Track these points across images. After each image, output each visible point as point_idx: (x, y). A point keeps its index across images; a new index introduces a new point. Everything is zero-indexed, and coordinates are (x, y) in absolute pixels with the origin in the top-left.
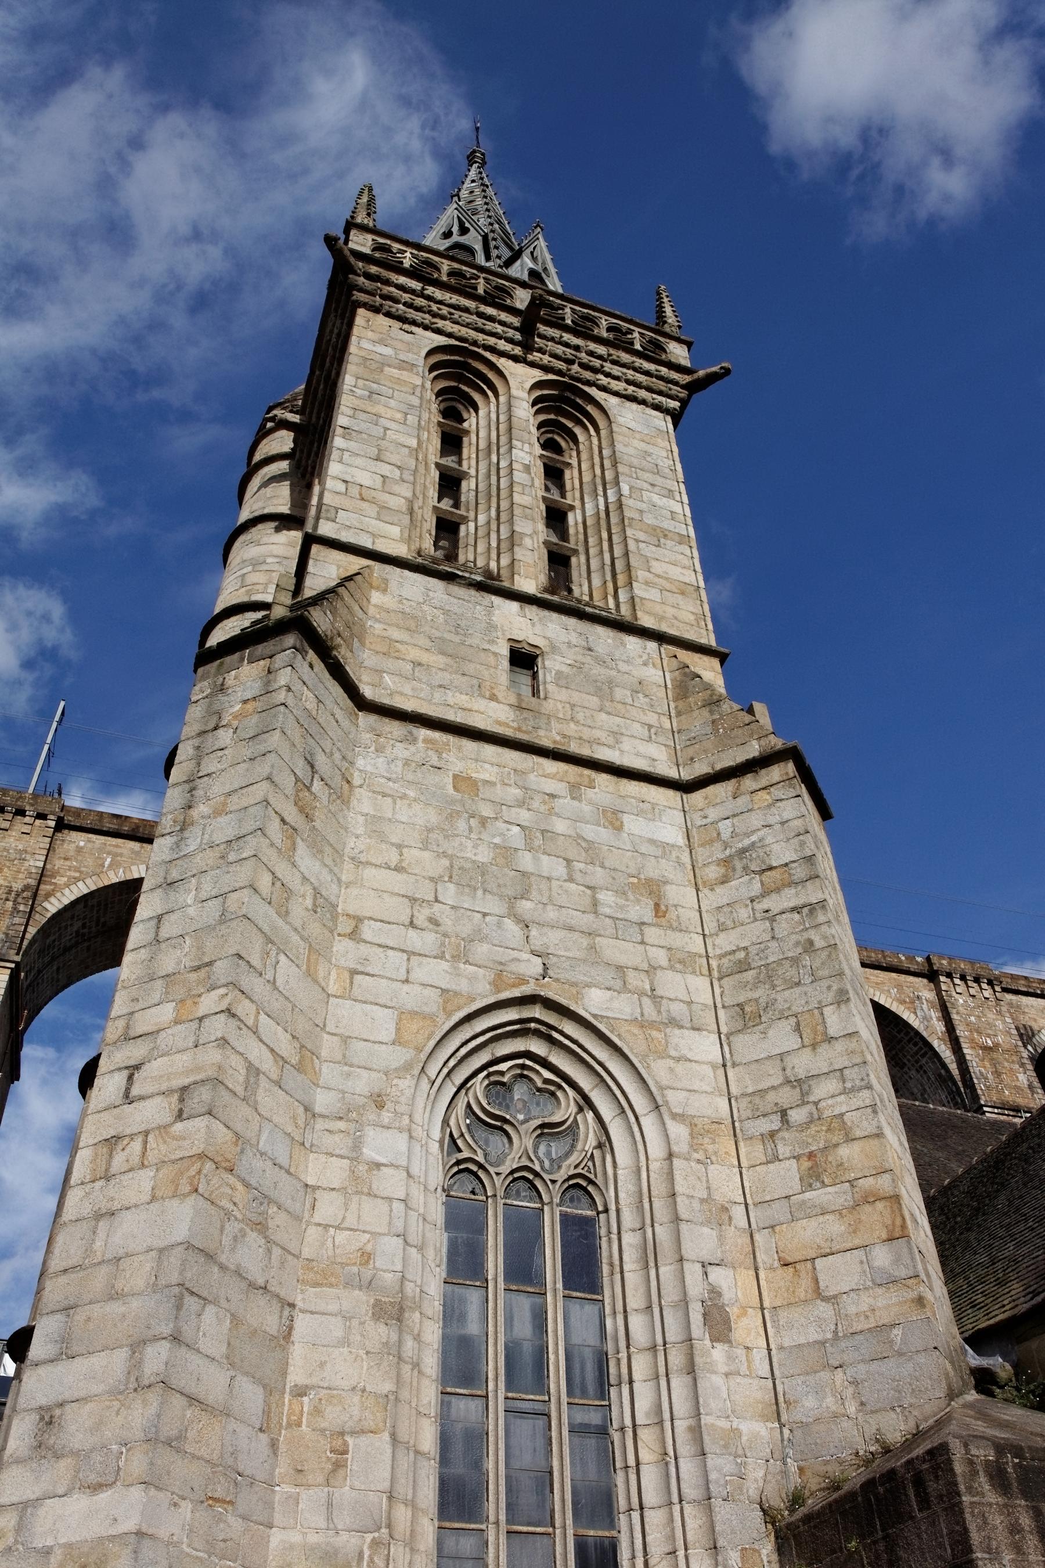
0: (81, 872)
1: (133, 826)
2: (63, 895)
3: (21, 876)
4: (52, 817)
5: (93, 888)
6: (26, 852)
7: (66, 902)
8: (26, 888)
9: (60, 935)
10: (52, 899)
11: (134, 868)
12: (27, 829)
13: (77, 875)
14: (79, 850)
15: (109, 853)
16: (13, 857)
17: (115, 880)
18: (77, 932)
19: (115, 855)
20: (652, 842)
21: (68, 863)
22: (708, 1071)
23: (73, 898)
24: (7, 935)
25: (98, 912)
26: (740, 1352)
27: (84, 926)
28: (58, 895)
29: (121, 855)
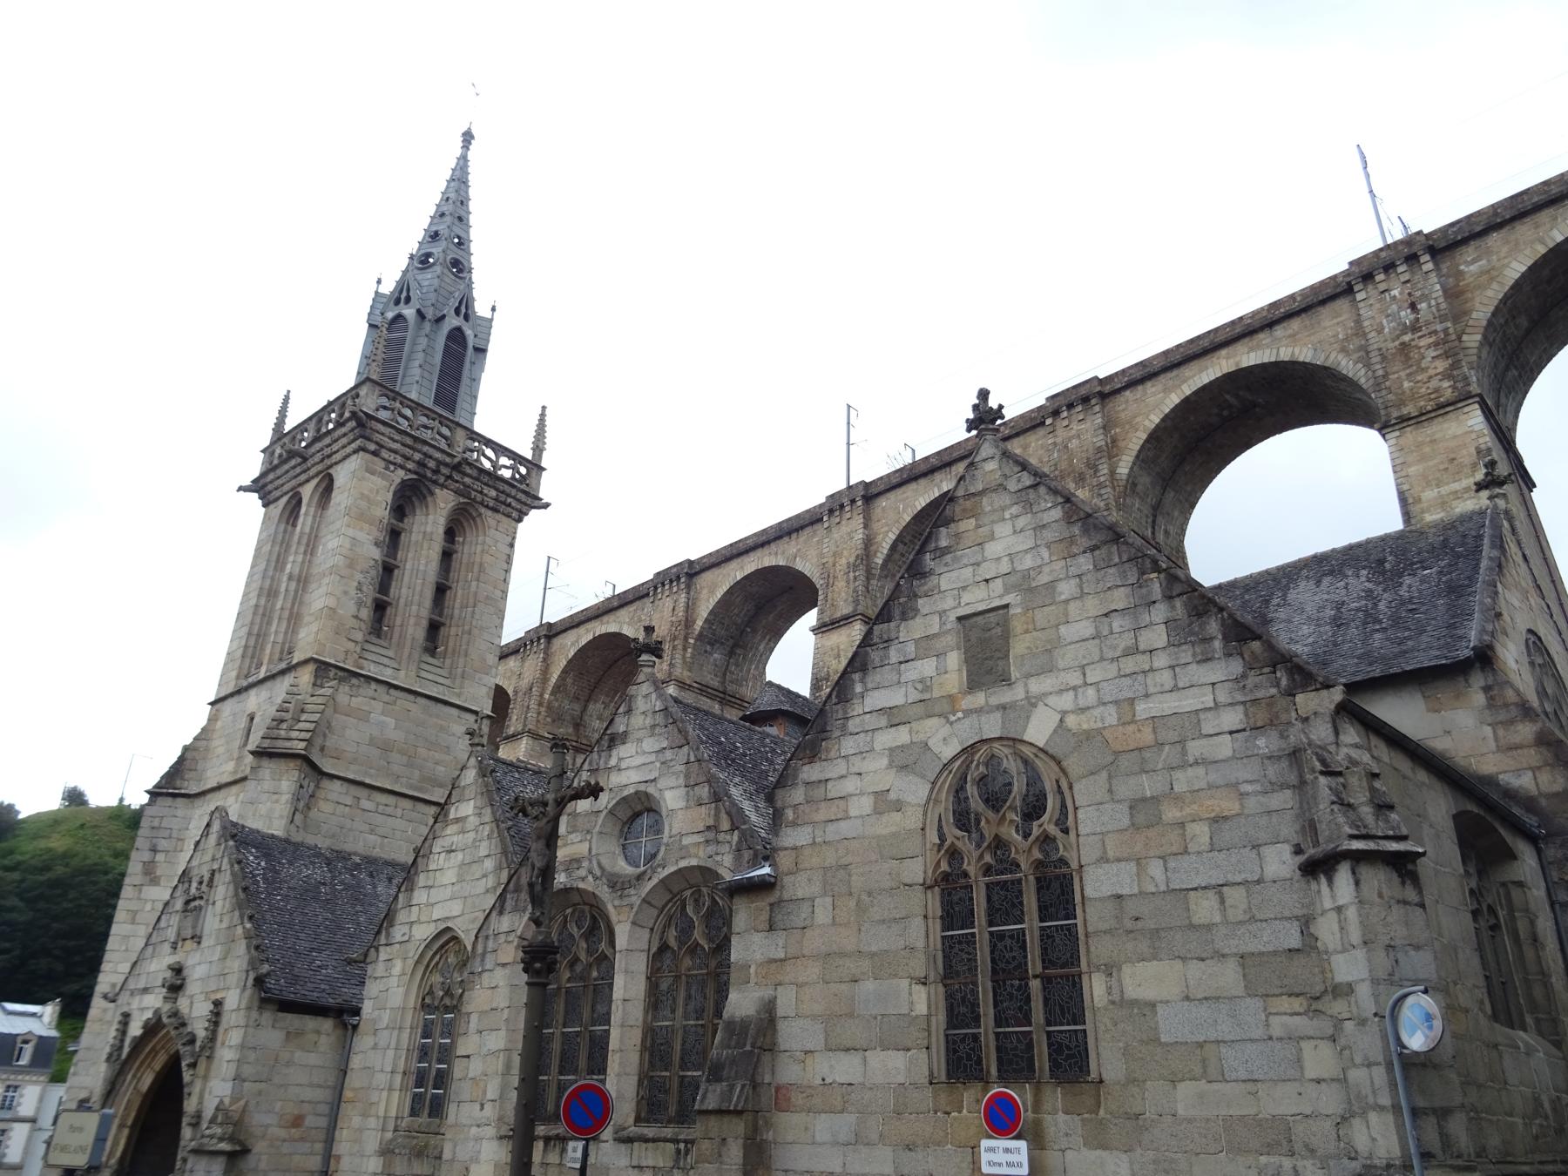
12: (848, 515)
14: (884, 509)
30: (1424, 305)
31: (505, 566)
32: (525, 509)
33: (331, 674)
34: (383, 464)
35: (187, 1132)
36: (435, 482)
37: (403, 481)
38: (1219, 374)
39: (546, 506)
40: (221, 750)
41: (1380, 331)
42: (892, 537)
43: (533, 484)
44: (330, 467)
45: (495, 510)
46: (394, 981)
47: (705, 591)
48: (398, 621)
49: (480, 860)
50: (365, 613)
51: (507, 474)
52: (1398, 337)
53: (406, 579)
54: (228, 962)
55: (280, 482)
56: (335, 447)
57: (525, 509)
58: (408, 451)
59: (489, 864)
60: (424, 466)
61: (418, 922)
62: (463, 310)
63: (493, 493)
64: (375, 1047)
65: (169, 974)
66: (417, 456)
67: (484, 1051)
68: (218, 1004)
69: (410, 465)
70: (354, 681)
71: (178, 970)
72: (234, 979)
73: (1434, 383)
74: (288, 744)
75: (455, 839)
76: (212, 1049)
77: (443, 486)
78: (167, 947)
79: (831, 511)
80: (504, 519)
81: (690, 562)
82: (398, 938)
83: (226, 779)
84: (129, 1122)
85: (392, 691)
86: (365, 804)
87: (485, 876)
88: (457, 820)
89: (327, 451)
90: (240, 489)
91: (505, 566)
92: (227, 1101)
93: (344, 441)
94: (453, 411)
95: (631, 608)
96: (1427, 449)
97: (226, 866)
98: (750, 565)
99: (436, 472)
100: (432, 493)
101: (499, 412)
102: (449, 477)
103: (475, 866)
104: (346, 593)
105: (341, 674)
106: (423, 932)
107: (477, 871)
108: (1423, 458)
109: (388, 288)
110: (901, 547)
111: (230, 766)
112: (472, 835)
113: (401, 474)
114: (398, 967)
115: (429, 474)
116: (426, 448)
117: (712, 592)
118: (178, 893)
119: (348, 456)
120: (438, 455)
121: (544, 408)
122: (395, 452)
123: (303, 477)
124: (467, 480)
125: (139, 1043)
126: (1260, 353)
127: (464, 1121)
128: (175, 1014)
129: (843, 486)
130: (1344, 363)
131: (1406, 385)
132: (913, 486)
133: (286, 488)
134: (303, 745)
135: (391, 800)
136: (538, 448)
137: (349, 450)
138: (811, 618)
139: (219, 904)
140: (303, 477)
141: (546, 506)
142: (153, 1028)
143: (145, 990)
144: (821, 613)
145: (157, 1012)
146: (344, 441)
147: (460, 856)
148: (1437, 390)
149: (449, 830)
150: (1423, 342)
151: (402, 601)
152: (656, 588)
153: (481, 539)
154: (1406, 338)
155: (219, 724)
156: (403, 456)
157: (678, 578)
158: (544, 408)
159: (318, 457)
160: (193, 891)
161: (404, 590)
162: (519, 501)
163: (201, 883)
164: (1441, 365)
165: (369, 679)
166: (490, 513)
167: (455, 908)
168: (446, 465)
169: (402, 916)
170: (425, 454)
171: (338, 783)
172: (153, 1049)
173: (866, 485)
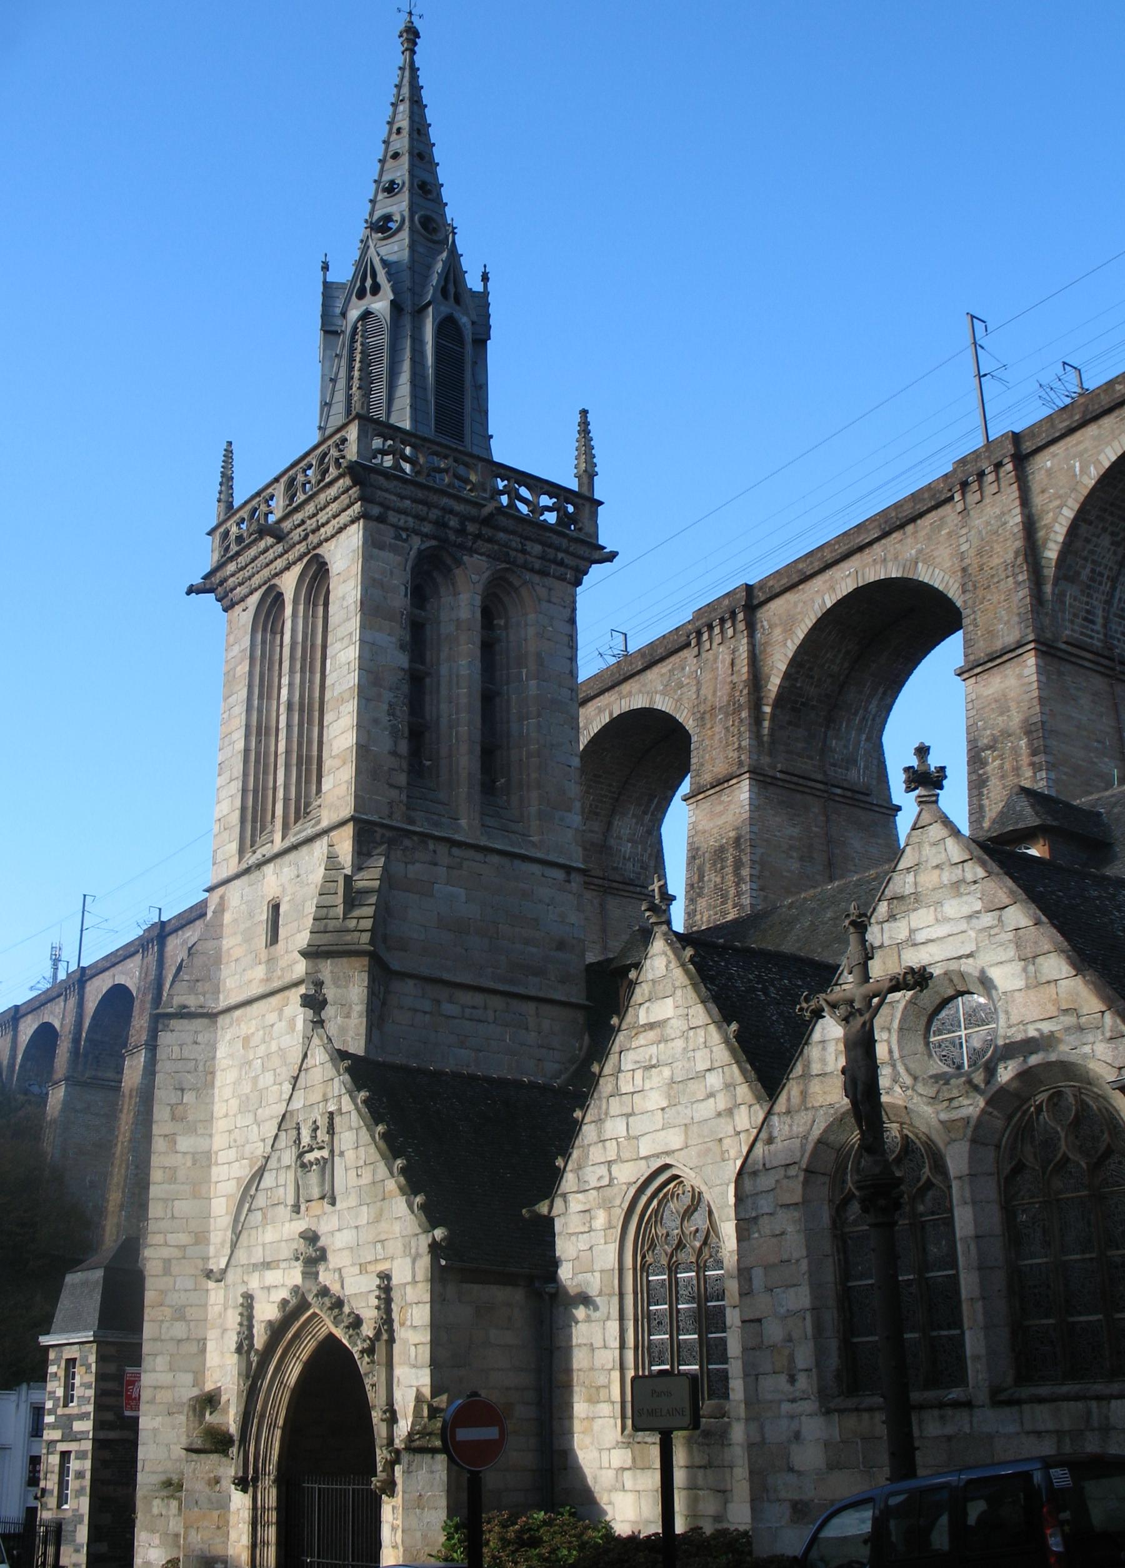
0: (1060, 497)
1: (1082, 409)
2: (1056, 532)
3: (1009, 543)
4: (1006, 460)
5: (1076, 507)
6: (1003, 514)
7: (1061, 539)
8: (1017, 554)
9: (1094, 562)
10: (1051, 545)
11: (1102, 457)
12: (994, 488)
13: (1057, 503)
14: (1049, 472)
15: (1074, 457)
16: (995, 527)
17: (1092, 483)
18: (1112, 544)
19: (1080, 455)
21: (1046, 495)
23: (1064, 530)
24: (1019, 614)
25: (1112, 514)
27: (1113, 534)
28: (1052, 535)
29: (1086, 450)
31: (568, 653)
32: (582, 564)
33: (378, 837)
34: (391, 532)
35: (380, 1430)
36: (461, 546)
37: (420, 552)
39: (612, 557)
40: (237, 952)
42: (1068, 514)
43: (588, 528)
44: (320, 544)
45: (543, 573)
46: (598, 1237)
47: (778, 631)
48: (444, 752)
49: (701, 1076)
50: (403, 747)
51: (551, 518)
53: (444, 691)
54: (384, 1225)
55: (246, 573)
56: (322, 517)
57: (582, 564)
58: (421, 509)
59: (714, 1080)
60: (445, 525)
61: (619, 1159)
62: (452, 290)
63: (537, 549)
65: (301, 1245)
66: (434, 514)
67: (782, 1310)
68: (385, 1277)
69: (427, 528)
70: (407, 842)
71: (311, 1238)
72: (395, 1247)
74: (348, 938)
76: (391, 1332)
77: (471, 551)
78: (284, 1212)
79: (964, 485)
80: (558, 584)
81: (749, 588)
82: (594, 1183)
83: (256, 990)
84: (281, 1423)
85: (456, 851)
86: (448, 1008)
87: (711, 1095)
88: (651, 1026)
89: (311, 524)
90: (191, 590)
91: (568, 653)
92: (427, 1392)
93: (334, 507)
94: (460, 438)
95: (663, 668)
97: (347, 1104)
98: (843, 581)
99: (462, 531)
100: (459, 563)
101: (525, 432)
102: (478, 536)
103: (693, 1086)
104: (376, 721)
105: (389, 834)
106: (629, 1174)
107: (697, 1089)
109: (343, 273)
110: (1084, 528)
111: (260, 972)
112: (679, 1044)
113: (416, 542)
114: (600, 1219)
115: (452, 537)
116: (445, 501)
117: (789, 631)
118: (282, 1142)
119: (340, 530)
120: (459, 507)
121: (584, 413)
122: (404, 512)
123: (279, 564)
124: (501, 535)
125: (277, 1330)
127: (769, 1397)
128: (324, 1292)
129: (978, 442)
132: (1092, 430)
133: (256, 580)
134: (366, 937)
135: (479, 999)
136: (588, 475)
137: (344, 518)
138: (950, 652)
139: (350, 1155)
140: (279, 564)
141: (612, 557)
142: (294, 1311)
143: (267, 1265)
144: (968, 643)
145: (296, 1290)
146: (334, 507)
147: (666, 1072)
149: (642, 1040)
151: (444, 721)
152: (699, 634)
153: (532, 617)
155: (227, 917)
156: (417, 517)
157: (733, 615)
158: (584, 413)
159: (296, 535)
160: (306, 1140)
161: (444, 706)
162: (572, 554)
163: (315, 1129)
165: (425, 837)
166: (536, 578)
167: (674, 1139)
168: (473, 519)
170: (443, 509)
171: (411, 982)
173: (1016, 438)
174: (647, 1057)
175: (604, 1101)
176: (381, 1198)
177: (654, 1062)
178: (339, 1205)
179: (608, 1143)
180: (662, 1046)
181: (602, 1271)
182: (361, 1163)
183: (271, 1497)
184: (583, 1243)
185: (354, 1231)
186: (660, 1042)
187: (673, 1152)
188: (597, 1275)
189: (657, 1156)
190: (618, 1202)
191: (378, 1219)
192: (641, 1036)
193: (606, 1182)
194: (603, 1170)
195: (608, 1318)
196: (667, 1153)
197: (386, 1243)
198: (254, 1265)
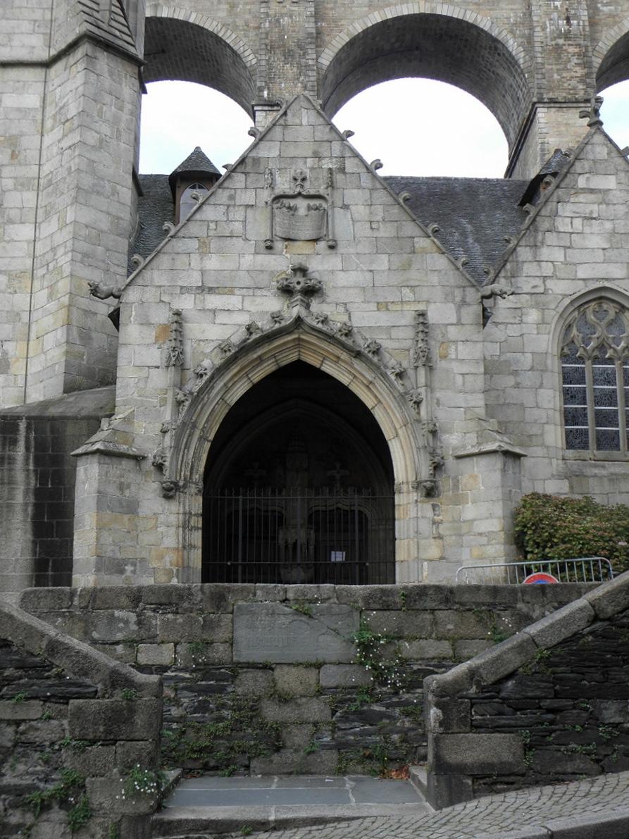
20: (19, 110)
22: (25, 245)
26: (12, 378)
30: (575, 22)
38: (417, 12)
41: (544, 29)
52: (555, 38)
64: (517, 386)
73: (573, 82)
75: (595, 207)
82: (527, 289)
84: (211, 437)
88: (592, 191)
96: (563, 129)
106: (564, 289)
108: (560, 134)
126: (451, 8)
130: (511, 42)
131: (556, 76)
148: (574, 89)
149: (582, 198)
150: (571, 49)
154: (561, 41)
164: (580, 71)
169: (529, 269)
172: (260, 357)
174: (588, 211)
175: (540, 234)
176: (409, 251)
177: (594, 216)
178: (341, 249)
179: (543, 264)
180: (603, 207)
181: (533, 353)
182: (379, 218)
183: (197, 504)
184: (513, 331)
185: (369, 275)
186: (601, 203)
187: (614, 279)
188: (529, 356)
189: (598, 280)
190: (553, 306)
191: (406, 267)
192: (582, 196)
193: (541, 290)
194: (539, 282)
195: (541, 386)
196: (607, 279)
197: (418, 289)
198: (182, 288)
